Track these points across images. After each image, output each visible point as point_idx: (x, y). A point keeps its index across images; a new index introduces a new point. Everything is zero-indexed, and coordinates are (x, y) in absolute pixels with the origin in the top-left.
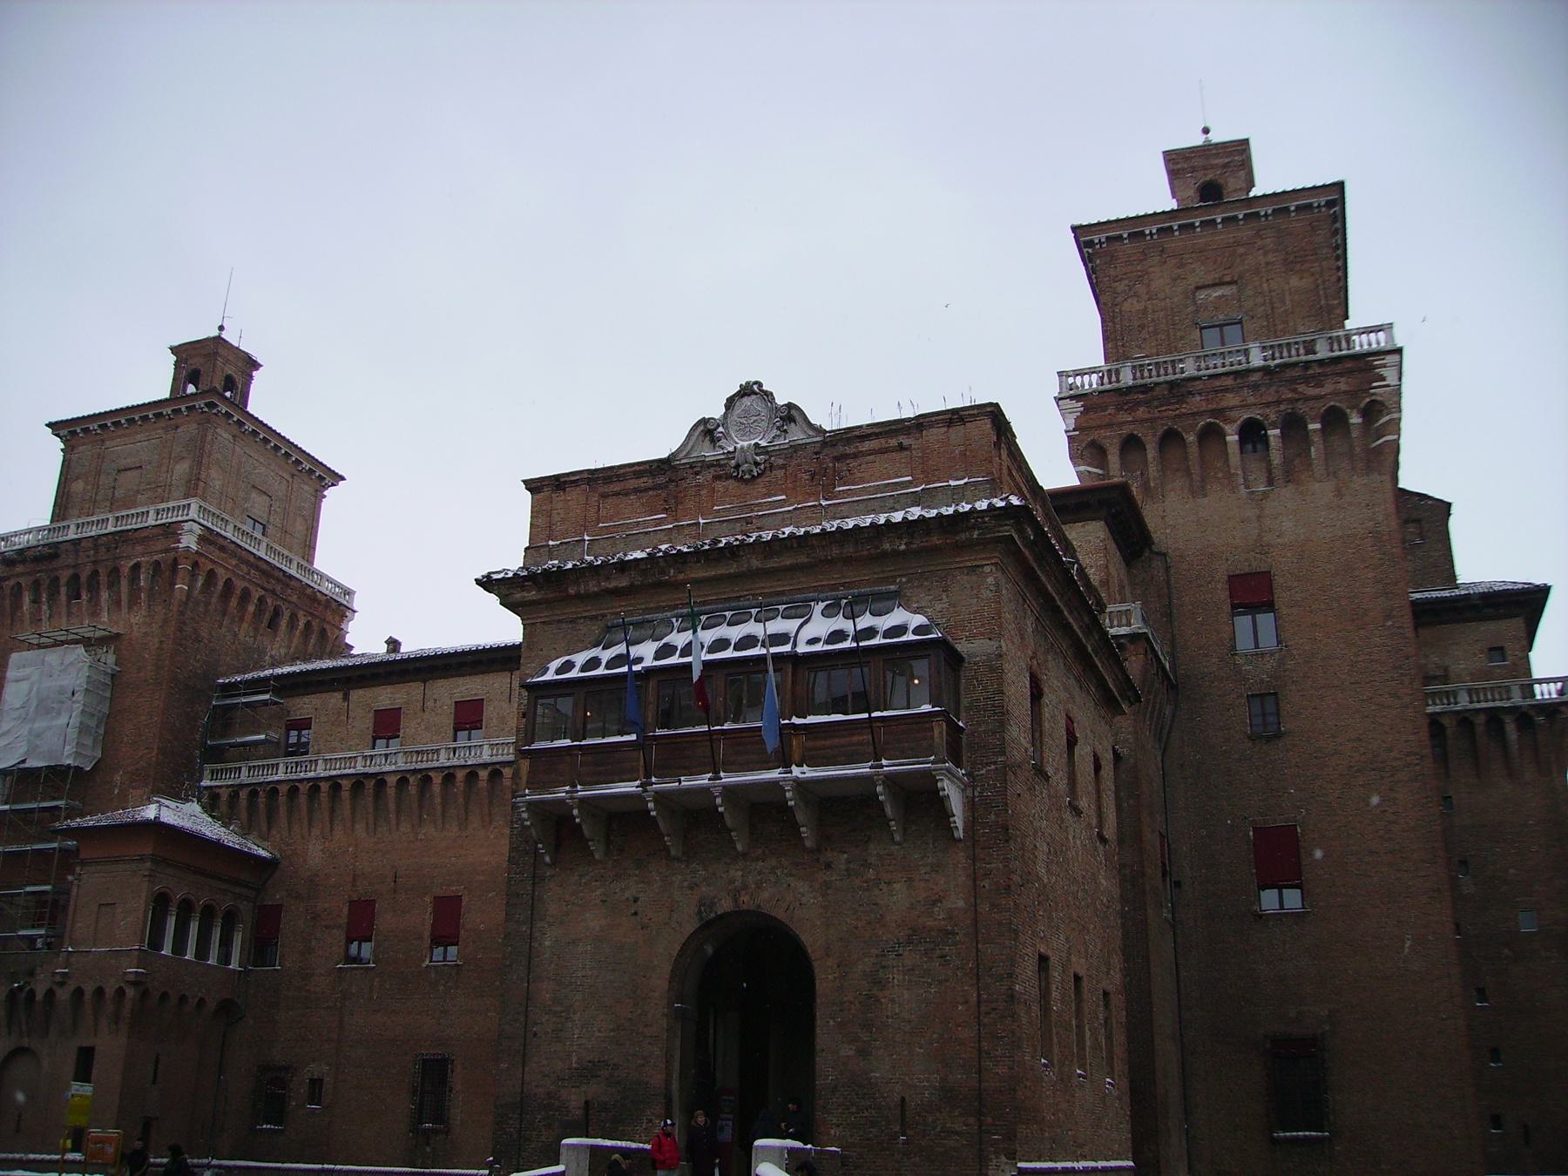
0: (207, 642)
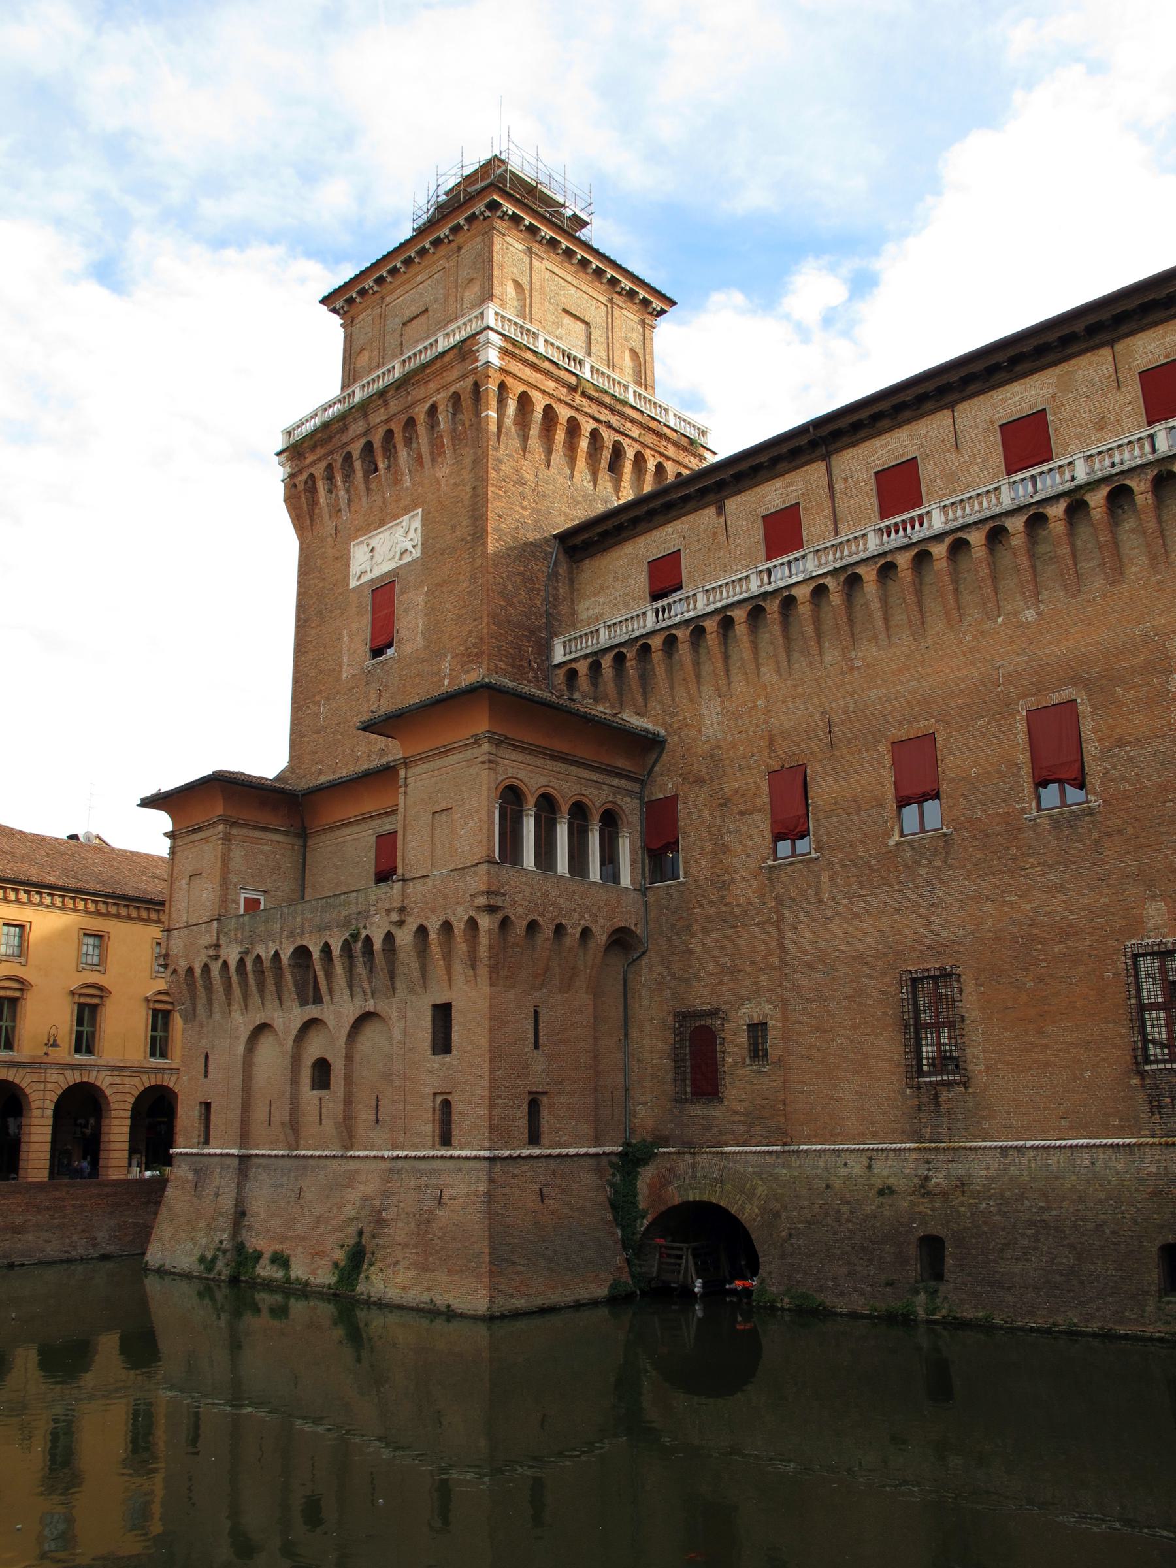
0: (533, 485)
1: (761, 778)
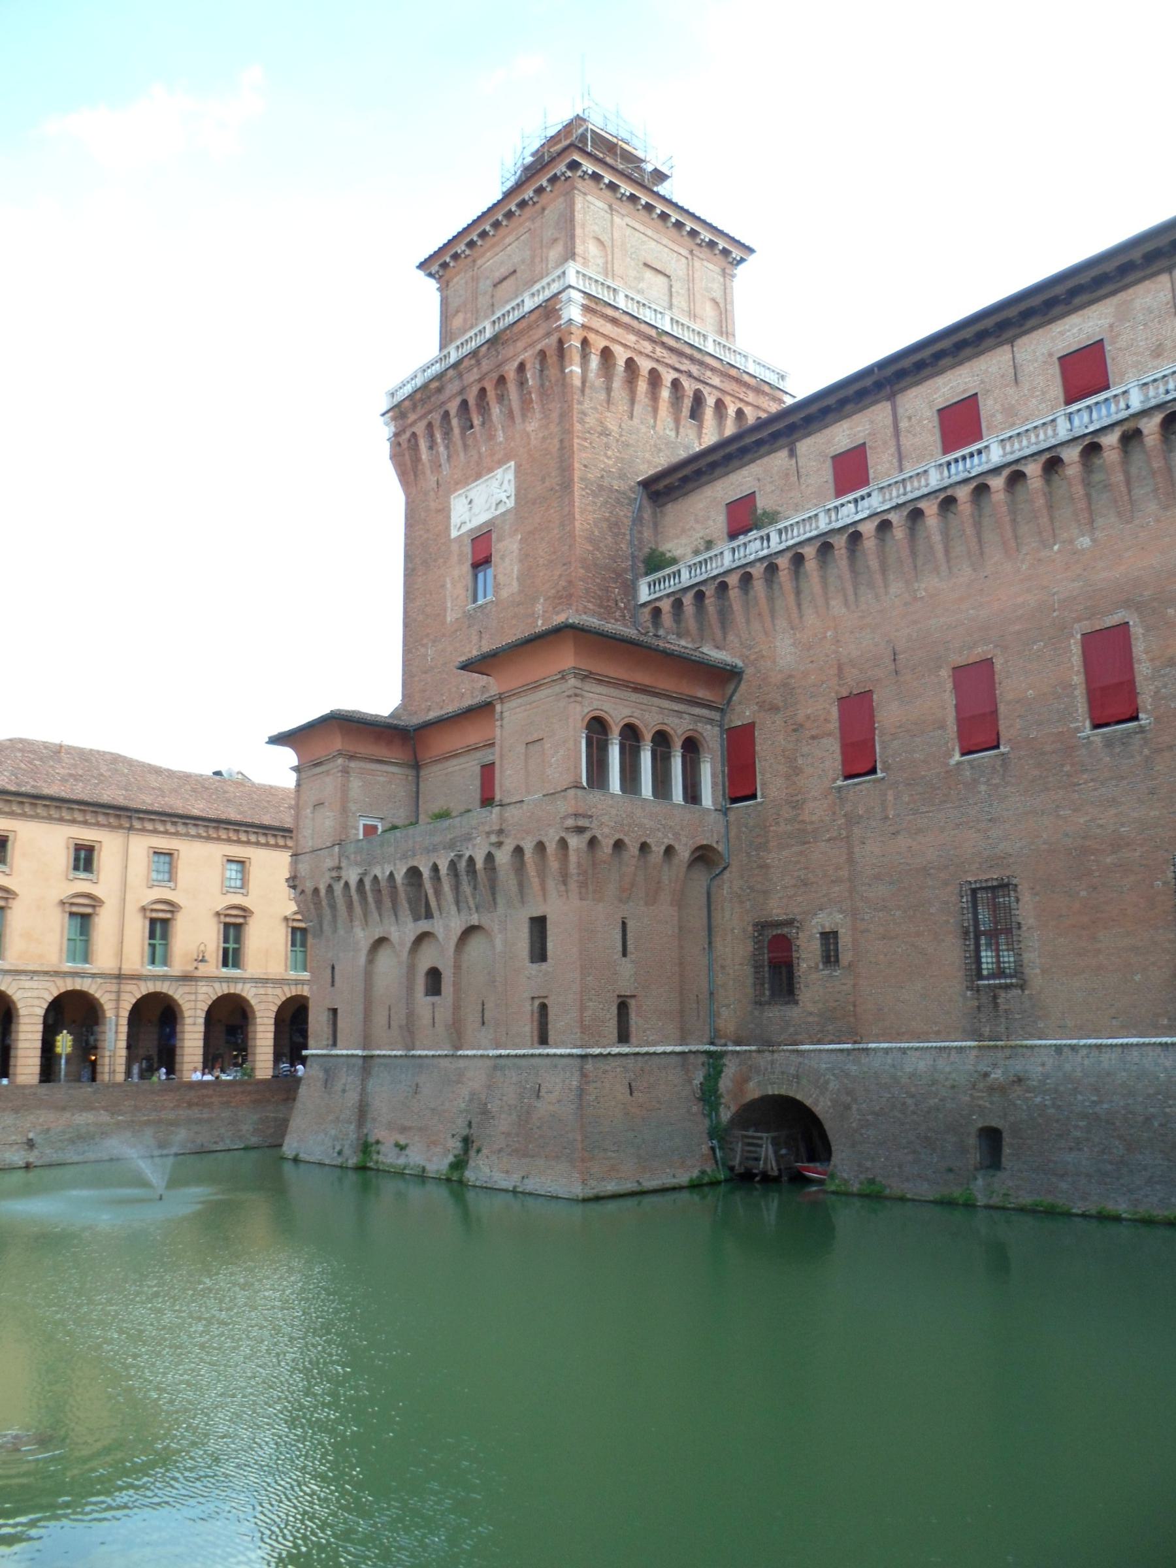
0: (617, 436)
1: (831, 704)
